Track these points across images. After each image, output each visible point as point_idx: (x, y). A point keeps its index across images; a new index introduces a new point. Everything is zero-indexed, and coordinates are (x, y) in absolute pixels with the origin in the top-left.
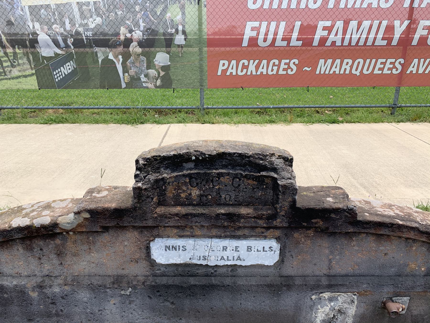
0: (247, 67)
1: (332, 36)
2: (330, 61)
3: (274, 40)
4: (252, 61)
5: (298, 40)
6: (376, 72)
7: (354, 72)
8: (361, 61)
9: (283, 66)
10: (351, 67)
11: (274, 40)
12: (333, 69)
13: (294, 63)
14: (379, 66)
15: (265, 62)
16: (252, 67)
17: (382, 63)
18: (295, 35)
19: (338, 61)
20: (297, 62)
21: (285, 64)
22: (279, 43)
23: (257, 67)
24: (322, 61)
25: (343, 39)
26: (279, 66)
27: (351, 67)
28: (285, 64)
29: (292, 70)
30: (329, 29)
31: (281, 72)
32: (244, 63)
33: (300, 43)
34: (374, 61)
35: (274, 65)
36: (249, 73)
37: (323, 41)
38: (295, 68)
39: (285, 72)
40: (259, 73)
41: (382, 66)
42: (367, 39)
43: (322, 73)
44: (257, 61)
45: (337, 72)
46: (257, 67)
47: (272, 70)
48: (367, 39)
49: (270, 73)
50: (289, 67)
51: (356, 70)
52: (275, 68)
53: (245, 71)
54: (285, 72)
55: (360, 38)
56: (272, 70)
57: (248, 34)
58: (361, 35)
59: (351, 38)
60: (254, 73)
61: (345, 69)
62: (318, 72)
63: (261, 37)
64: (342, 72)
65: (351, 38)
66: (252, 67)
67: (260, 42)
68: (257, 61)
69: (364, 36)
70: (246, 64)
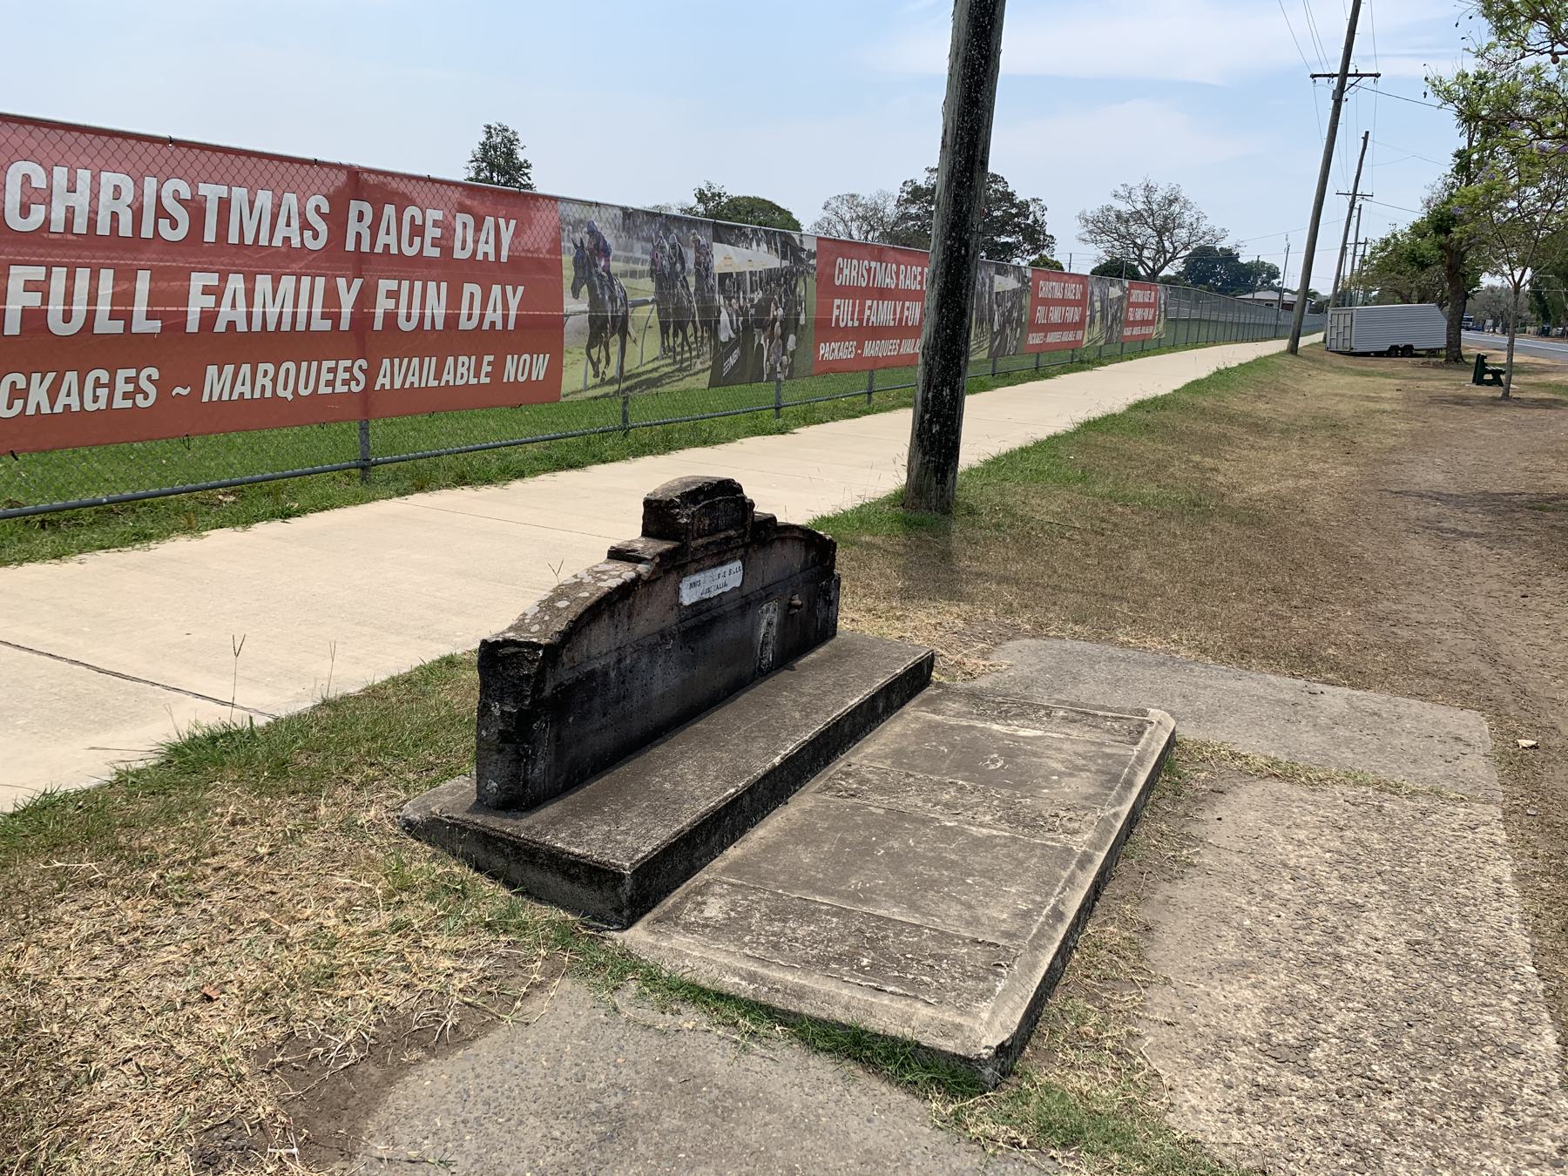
0: (24, 394)
1: (225, 308)
2: (229, 369)
3: (91, 316)
4: (36, 377)
5: (150, 316)
6: (323, 390)
7: (281, 393)
8: (291, 365)
9: (121, 387)
10: (274, 380)
11: (91, 316)
12: (238, 389)
13: (149, 378)
14: (325, 376)
15: (71, 377)
16: (38, 395)
17: (330, 370)
18: (140, 307)
19: (246, 368)
20: (364, 364)
21: (128, 380)
22: (104, 325)
23: (53, 393)
24: (212, 370)
25: (249, 316)
26: (111, 386)
27: (274, 380)
28: (128, 380)
29: (146, 397)
30: (217, 292)
31: (119, 403)
32: (14, 383)
33: (155, 326)
34: (315, 364)
35: (98, 384)
36: (31, 411)
37: (208, 318)
38: (152, 391)
39: (128, 404)
40: (58, 409)
41: (330, 377)
42: (295, 315)
43: (215, 398)
44: (51, 376)
45: (248, 396)
46: (53, 393)
47: (96, 399)
48: (295, 315)
49: (90, 406)
50: (138, 390)
51: (285, 388)
52: (103, 393)
53: (19, 404)
54: (128, 404)
55: (281, 313)
56: (96, 399)
57: (18, 300)
58: (282, 307)
59: (264, 313)
60: (46, 409)
61: (263, 387)
62: (205, 399)
63: (56, 307)
64: (257, 395)
65: (264, 313)
66: (38, 395)
67: (56, 326)
68: (51, 376)
69: (288, 310)
70: (21, 384)
